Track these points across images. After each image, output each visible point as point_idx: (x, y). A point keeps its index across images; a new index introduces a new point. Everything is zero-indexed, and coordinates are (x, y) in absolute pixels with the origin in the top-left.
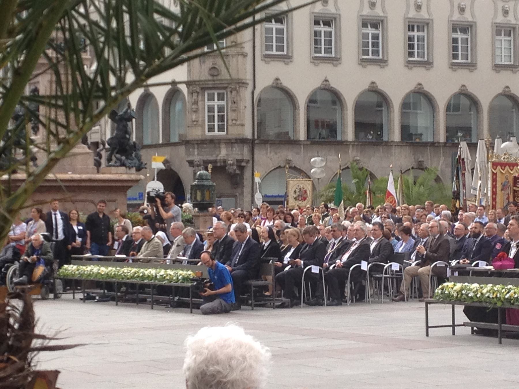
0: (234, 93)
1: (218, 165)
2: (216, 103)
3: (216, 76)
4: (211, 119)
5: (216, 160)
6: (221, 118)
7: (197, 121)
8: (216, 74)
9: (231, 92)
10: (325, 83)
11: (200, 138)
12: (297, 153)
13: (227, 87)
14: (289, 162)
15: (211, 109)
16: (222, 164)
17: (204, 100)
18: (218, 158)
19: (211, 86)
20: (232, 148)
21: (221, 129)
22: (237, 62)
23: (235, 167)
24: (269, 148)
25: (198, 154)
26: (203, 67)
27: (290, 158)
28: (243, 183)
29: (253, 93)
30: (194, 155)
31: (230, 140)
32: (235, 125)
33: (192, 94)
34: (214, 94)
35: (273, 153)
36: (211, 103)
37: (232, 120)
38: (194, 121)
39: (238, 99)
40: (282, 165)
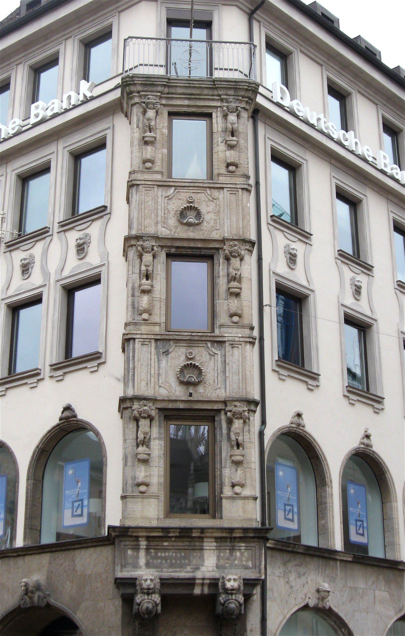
1: (197, 591)
3: (195, 384)
5: (194, 579)
7: (147, 485)
8: (194, 379)
18: (199, 575)
20: (232, 549)
22: (244, 357)
23: (241, 598)
25: (148, 565)
26: (163, 364)
27: (326, 586)
29: (261, 434)
30: (136, 566)
31: (231, 530)
32: (237, 496)
33: (137, 420)
37: (233, 486)
38: (139, 485)
39: (246, 438)
40: (312, 604)
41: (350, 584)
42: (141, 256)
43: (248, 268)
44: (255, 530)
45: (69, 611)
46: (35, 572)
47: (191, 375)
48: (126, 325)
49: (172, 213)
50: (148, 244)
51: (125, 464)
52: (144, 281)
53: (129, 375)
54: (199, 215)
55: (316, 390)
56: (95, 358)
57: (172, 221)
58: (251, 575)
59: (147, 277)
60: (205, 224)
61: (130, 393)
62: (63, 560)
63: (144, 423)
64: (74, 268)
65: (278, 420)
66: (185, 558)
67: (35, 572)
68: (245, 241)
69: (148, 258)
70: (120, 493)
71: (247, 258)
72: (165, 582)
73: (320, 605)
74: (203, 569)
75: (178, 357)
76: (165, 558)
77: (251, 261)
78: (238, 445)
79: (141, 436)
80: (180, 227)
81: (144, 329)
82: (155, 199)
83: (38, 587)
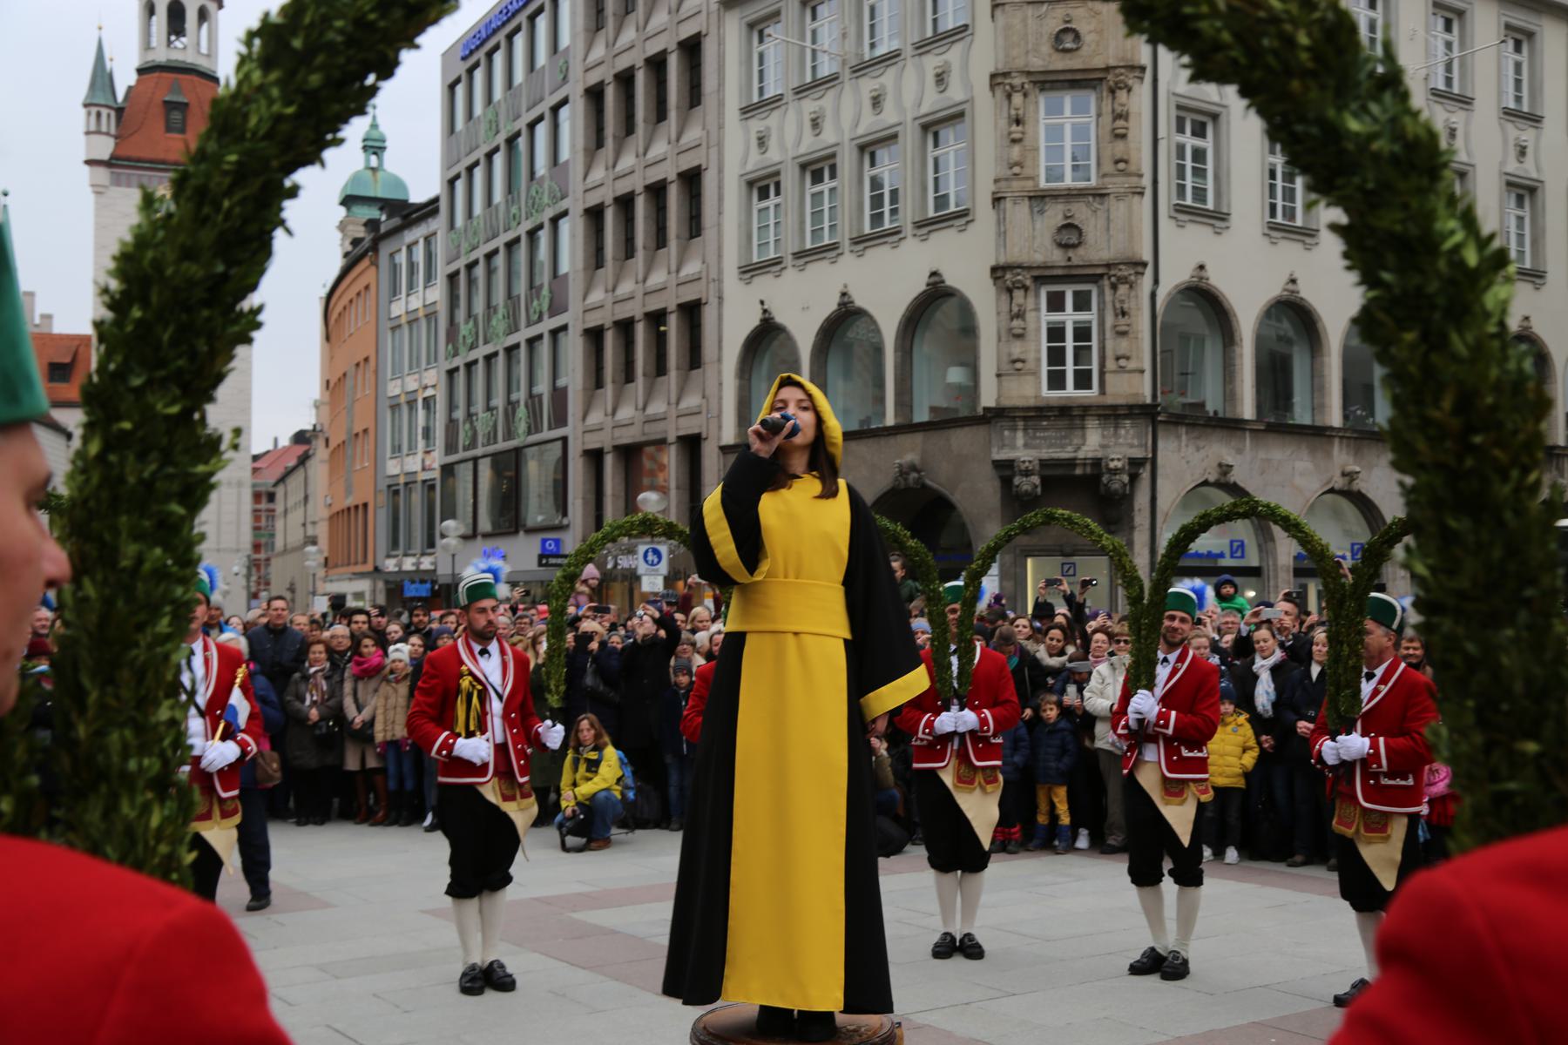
0: (1123, 289)
1: (1078, 471)
2: (1069, 318)
3: (1074, 246)
4: (1056, 356)
6: (1081, 354)
7: (1023, 361)
8: (1074, 240)
9: (1114, 287)
10: (1291, 287)
11: (1032, 403)
12: (1240, 451)
13: (1101, 276)
14: (1225, 469)
15: (1056, 333)
16: (1088, 470)
17: (1037, 309)
18: (1081, 455)
19: (1060, 272)
20: (1116, 427)
21: (1083, 380)
23: (1126, 478)
24: (1184, 437)
25: (1026, 445)
26: (1038, 225)
27: (1229, 460)
28: (1132, 519)
29: (1153, 296)
30: (1013, 447)
31: (1114, 407)
33: (1010, 291)
34: (1063, 293)
35: (1191, 449)
36: (1056, 317)
37: (1118, 359)
38: (1014, 362)
39: (1133, 304)
40: (1212, 479)
41: (1262, 455)
42: (1009, 96)
43: (1143, 91)
44: (1144, 407)
45: (946, 492)
46: (909, 451)
47: (1069, 236)
48: (996, 181)
49: (1046, 37)
50: (1017, 81)
51: (999, 340)
52: (1014, 128)
53: (1002, 234)
54: (1077, 36)
55: (1225, 233)
56: (964, 215)
57: (1046, 48)
58: (1138, 453)
59: (1018, 122)
60: (1085, 48)
61: (1002, 261)
62: (937, 440)
63: (1019, 294)
64: (932, 102)
65: (1175, 274)
66: (1065, 437)
67: (909, 451)
68: (1132, 68)
69: (1017, 99)
70: (994, 371)
71: (1136, 87)
72: (1044, 464)
73: (1223, 480)
74: (1085, 448)
75: (1055, 214)
76: (1044, 438)
77: (1143, 91)
78: (1124, 314)
79: (1015, 309)
80: (1057, 56)
81: (1016, 185)
82: (1024, 20)
83: (913, 468)
